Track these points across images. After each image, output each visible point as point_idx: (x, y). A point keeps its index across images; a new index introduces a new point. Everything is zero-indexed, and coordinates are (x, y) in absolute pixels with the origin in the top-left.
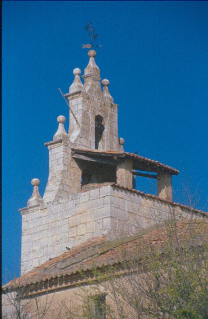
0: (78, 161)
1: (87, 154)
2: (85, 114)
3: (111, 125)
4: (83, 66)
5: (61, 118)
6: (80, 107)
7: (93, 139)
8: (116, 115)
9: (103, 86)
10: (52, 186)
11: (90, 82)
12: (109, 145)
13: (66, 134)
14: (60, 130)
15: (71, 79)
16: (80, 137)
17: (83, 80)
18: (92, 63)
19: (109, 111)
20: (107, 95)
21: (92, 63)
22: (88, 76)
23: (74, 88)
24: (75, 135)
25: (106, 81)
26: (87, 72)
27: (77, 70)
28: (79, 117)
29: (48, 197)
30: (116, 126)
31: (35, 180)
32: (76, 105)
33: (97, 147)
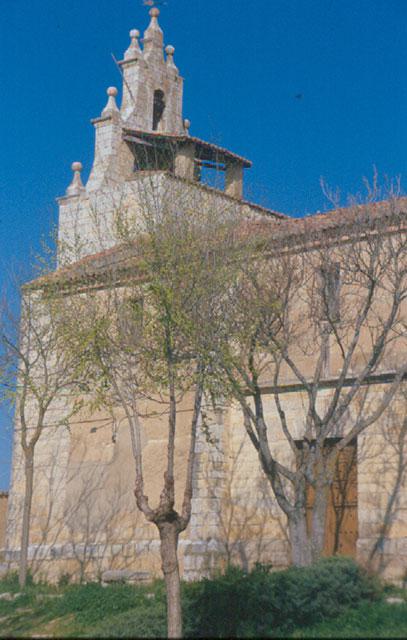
0: (130, 143)
1: (147, 137)
2: (141, 88)
3: (174, 103)
4: (143, 26)
5: (111, 90)
6: (136, 78)
7: (151, 120)
8: (180, 94)
9: (166, 54)
10: (97, 174)
11: (150, 48)
12: (171, 125)
13: (117, 110)
14: (111, 104)
15: (127, 42)
16: (135, 114)
17: (141, 45)
18: (153, 25)
19: (173, 85)
20: (171, 65)
21: (153, 25)
22: (149, 41)
23: (129, 54)
24: (128, 110)
25: (170, 48)
26: (147, 35)
27: (134, 33)
28: (134, 89)
29: (93, 184)
30: (180, 104)
31: (76, 165)
32: (132, 75)
33: (155, 128)
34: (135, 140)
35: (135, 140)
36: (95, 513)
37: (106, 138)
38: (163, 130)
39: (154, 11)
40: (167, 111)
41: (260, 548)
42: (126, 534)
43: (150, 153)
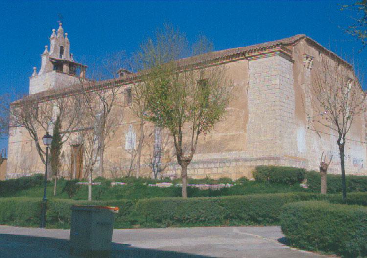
0: (51, 61)
1: (58, 61)
2: (56, 45)
3: (67, 49)
4: (57, 29)
5: (46, 46)
6: (54, 43)
7: (59, 54)
8: (69, 47)
9: (64, 36)
10: (42, 70)
11: (59, 35)
12: (66, 57)
13: (48, 52)
14: (46, 50)
15: (51, 33)
16: (53, 53)
17: (56, 33)
18: (60, 28)
19: (66, 44)
20: (66, 39)
21: (60, 28)
22: (59, 32)
23: (52, 36)
24: (52, 52)
25: (66, 34)
26: (58, 31)
27: (54, 30)
28: (54, 46)
29: (40, 73)
30: (69, 50)
31: (35, 68)
32: (53, 42)
33: (61, 56)
34: (53, 61)
35: (53, 61)
36: (27, 165)
37: (44, 59)
38: (63, 57)
39: (60, 24)
40: (64, 52)
41: (63, 173)
42: (34, 170)
43: (58, 65)
